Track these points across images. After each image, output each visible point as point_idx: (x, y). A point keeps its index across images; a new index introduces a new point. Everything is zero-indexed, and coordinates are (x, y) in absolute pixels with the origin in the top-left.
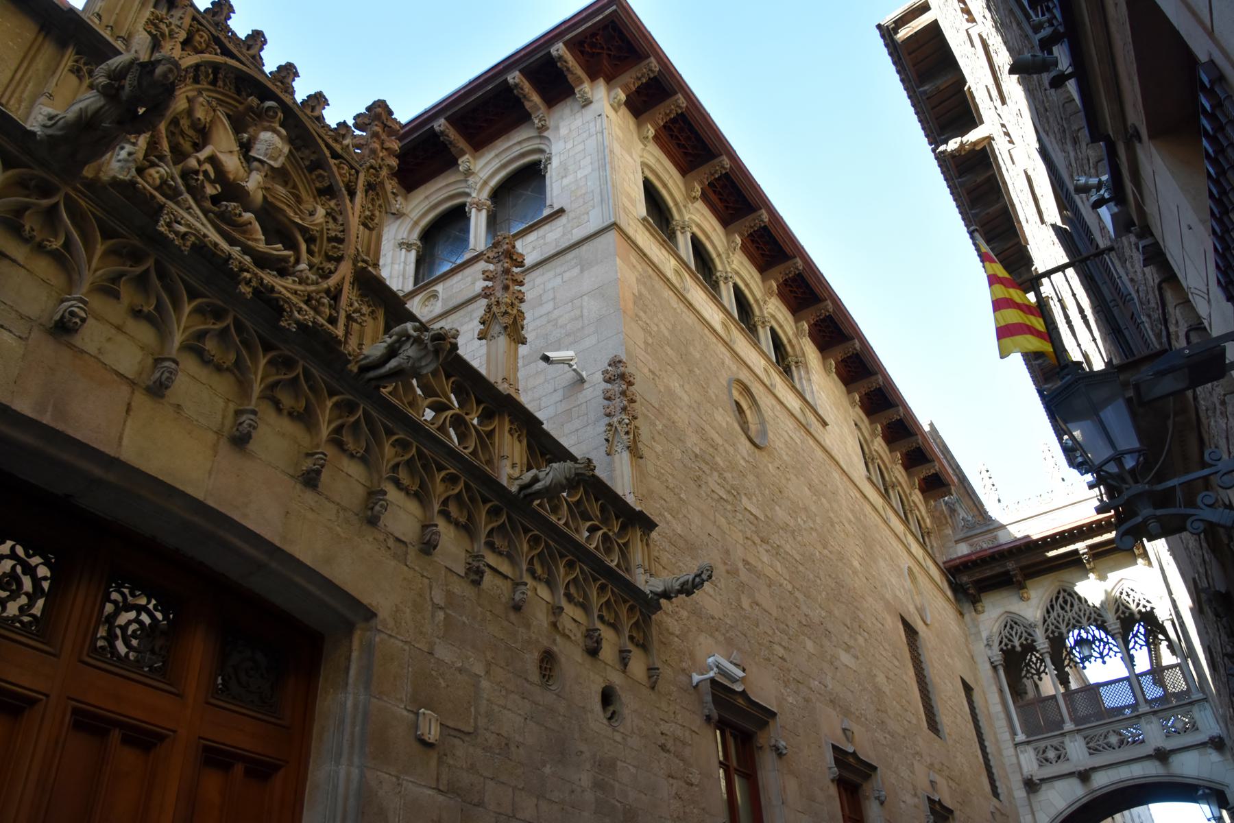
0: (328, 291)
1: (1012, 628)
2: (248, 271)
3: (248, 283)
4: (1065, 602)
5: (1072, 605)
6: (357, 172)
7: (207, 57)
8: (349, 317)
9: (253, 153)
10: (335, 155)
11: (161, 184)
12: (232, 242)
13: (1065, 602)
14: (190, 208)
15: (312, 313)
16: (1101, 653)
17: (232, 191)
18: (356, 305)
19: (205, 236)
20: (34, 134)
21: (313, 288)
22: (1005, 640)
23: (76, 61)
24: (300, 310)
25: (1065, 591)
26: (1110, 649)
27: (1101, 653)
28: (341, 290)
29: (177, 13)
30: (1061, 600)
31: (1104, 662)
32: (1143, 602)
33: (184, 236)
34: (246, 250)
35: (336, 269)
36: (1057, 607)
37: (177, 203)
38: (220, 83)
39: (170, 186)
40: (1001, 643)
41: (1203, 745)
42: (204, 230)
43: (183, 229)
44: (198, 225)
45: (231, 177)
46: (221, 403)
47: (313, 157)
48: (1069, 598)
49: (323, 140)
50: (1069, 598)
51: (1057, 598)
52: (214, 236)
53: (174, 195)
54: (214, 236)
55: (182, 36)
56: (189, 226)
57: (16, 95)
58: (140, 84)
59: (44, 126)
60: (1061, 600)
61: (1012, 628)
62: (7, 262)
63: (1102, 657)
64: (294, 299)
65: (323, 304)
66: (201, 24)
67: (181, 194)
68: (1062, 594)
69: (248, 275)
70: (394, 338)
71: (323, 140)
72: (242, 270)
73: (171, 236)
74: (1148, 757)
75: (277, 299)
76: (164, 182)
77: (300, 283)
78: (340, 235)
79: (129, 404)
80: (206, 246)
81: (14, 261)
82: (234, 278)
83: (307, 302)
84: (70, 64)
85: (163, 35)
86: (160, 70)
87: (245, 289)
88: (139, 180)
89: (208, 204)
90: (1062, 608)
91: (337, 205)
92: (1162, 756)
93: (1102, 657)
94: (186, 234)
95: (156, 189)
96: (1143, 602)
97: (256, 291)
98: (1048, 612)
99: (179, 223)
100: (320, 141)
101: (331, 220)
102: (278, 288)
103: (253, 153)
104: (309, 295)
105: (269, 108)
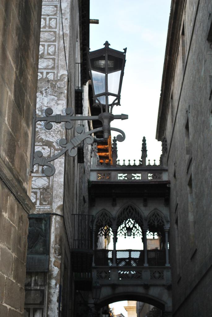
1: (104, 216)
4: (130, 211)
5: (132, 214)
13: (130, 211)
16: (134, 233)
22: (99, 221)
25: (131, 207)
26: (138, 232)
27: (134, 233)
30: (128, 210)
31: (134, 238)
32: (160, 221)
36: (126, 213)
40: (97, 222)
41: (164, 285)
48: (131, 210)
50: (131, 210)
51: (127, 209)
60: (128, 210)
61: (104, 216)
63: (134, 235)
68: (130, 208)
74: (141, 285)
90: (128, 214)
92: (147, 287)
93: (134, 235)
96: (160, 221)
98: (121, 214)
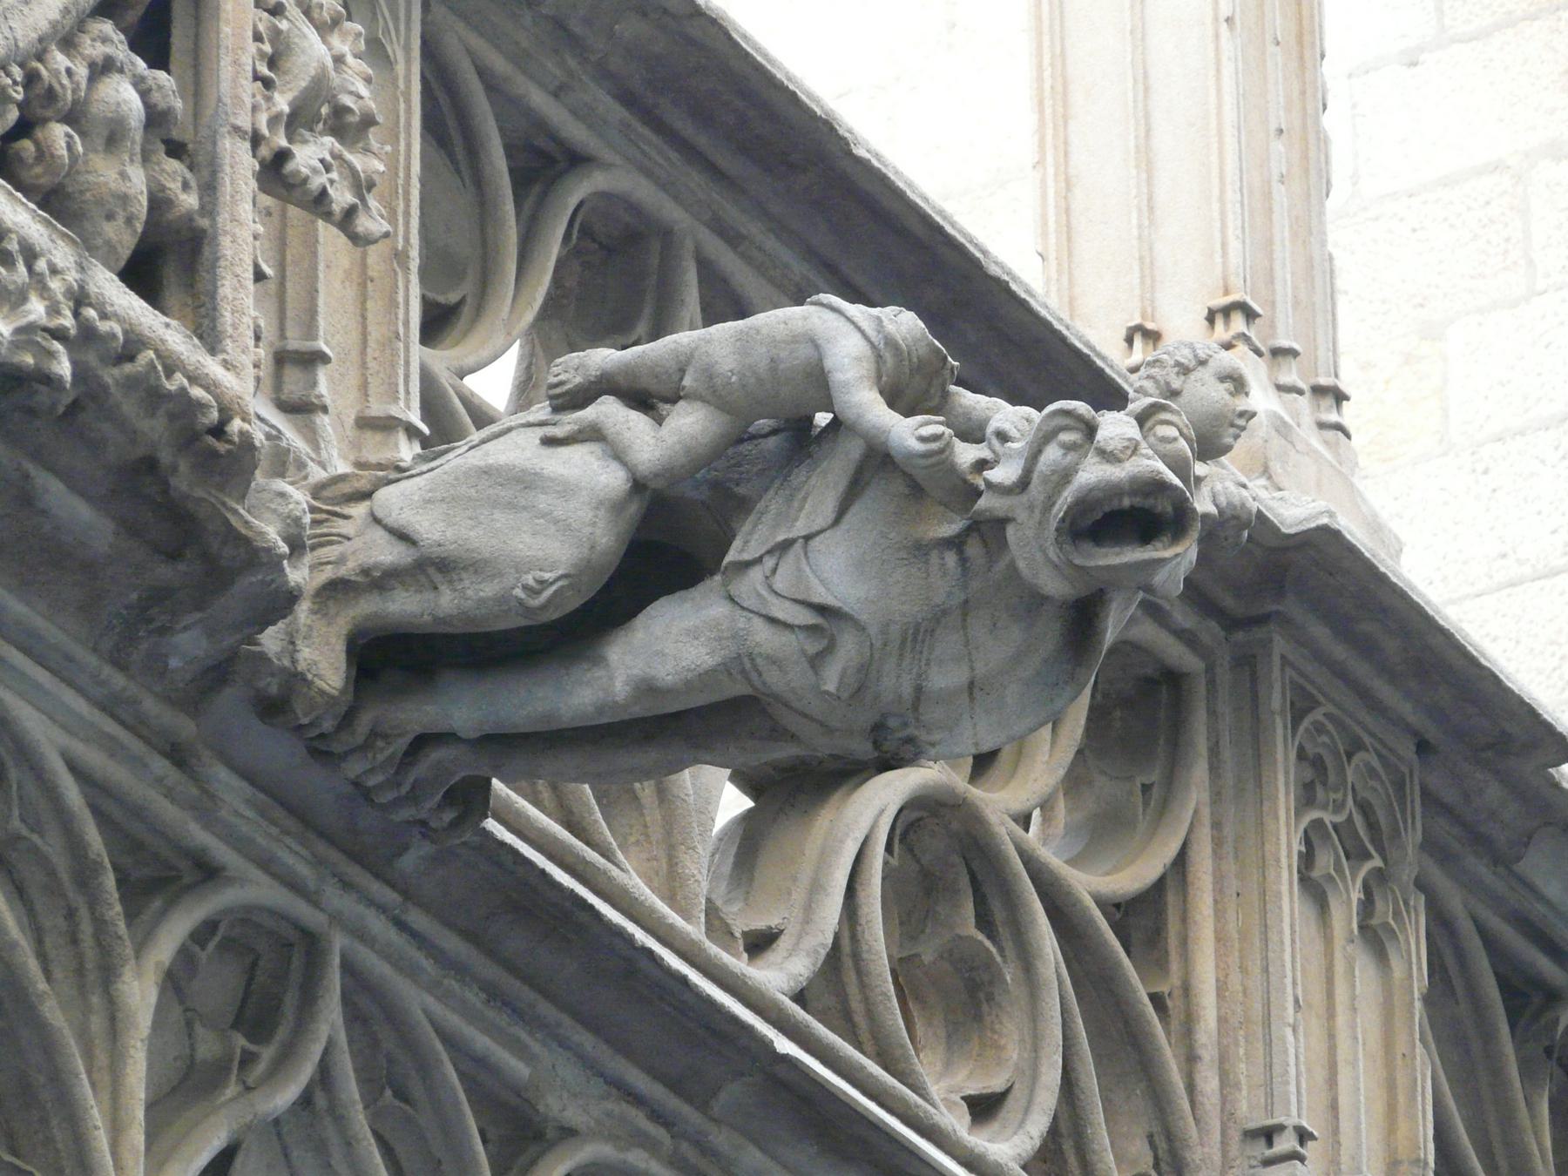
15: (60, 253)
18: (313, 50)
65: (113, 137)
70: (688, 424)
104: (31, 79)
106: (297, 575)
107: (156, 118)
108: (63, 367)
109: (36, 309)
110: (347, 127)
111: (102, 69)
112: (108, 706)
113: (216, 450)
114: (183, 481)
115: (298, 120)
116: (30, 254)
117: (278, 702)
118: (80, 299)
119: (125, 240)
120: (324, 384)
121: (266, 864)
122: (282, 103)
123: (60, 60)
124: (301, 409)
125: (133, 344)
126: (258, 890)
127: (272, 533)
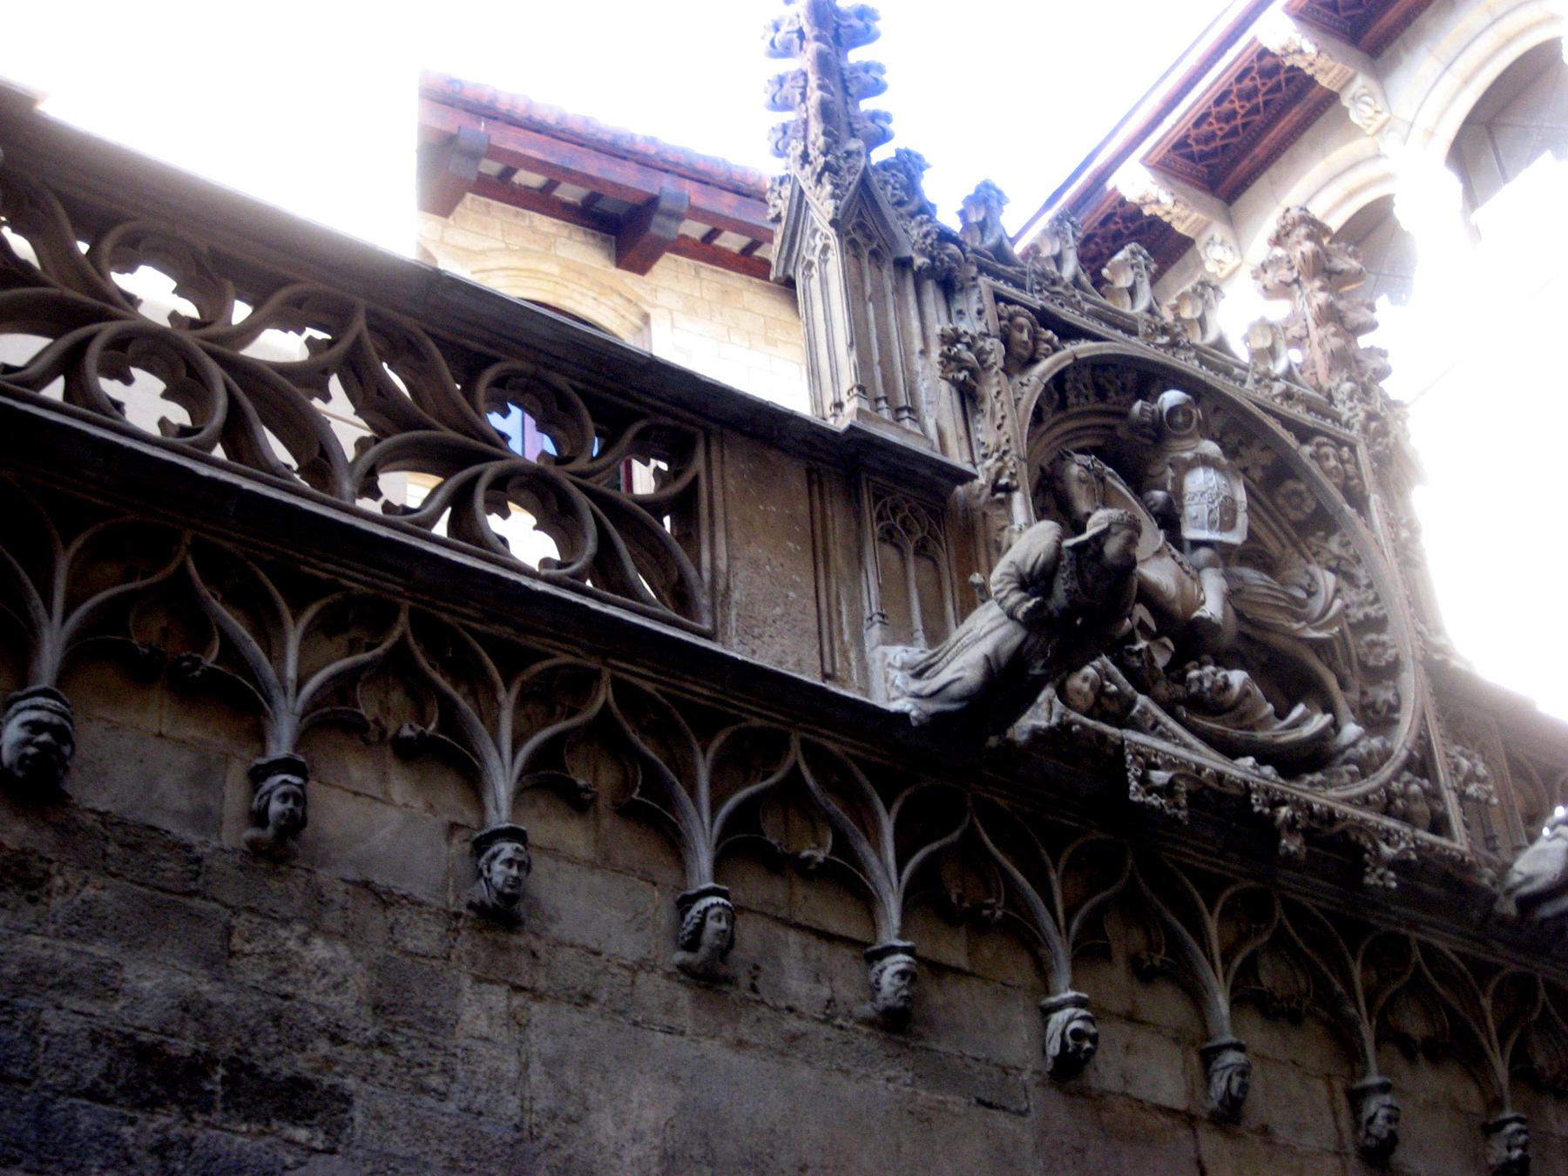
0: (1408, 765)
2: (1283, 803)
3: (1291, 825)
6: (1353, 449)
7: (1045, 367)
8: (1463, 797)
9: (1190, 533)
10: (1305, 434)
11: (1097, 702)
12: (1231, 750)
14: (1157, 723)
17: (1192, 638)
18: (1465, 764)
19: (1200, 769)
20: (903, 717)
21: (1386, 772)
23: (880, 518)
24: (1388, 835)
28: (1429, 744)
29: (970, 303)
33: (1168, 790)
34: (1266, 754)
35: (1397, 695)
37: (1136, 726)
38: (1072, 399)
39: (1111, 696)
42: (1196, 758)
43: (1160, 777)
44: (1182, 752)
45: (1178, 607)
46: (1319, 1085)
47: (1266, 458)
49: (1276, 415)
52: (1212, 761)
53: (1122, 714)
54: (1212, 761)
55: (995, 347)
56: (1169, 764)
57: (837, 645)
58: (1083, 585)
59: (917, 696)
62: (949, 978)
64: (1372, 817)
66: (1009, 301)
67: (1132, 702)
69: (1284, 811)
71: (1276, 415)
72: (1275, 804)
73: (1154, 800)
75: (1344, 833)
76: (1100, 691)
77: (1364, 775)
78: (1371, 611)
79: (1199, 1162)
80: (1205, 786)
81: (957, 971)
82: (1267, 829)
83: (1387, 811)
84: (877, 530)
85: (972, 371)
86: (1112, 547)
87: (1291, 844)
88: (1074, 715)
89: (1162, 689)
91: (1345, 545)
94: (1172, 782)
95: (1088, 715)
97: (1309, 836)
99: (1156, 767)
100: (1271, 422)
101: (1344, 585)
102: (1342, 809)
103: (1190, 533)
104: (1388, 791)
105: (1173, 410)
106: (1497, 890)
107: (1425, 791)
108: (1413, 856)
109: (1403, 845)
110: (1480, 780)
111: (1407, 784)
112: (1460, 934)
113: (1462, 865)
114: (1458, 875)
115: (1467, 782)
116: (1398, 832)
117: (1503, 921)
118: (1414, 840)
119: (1427, 823)
120: (1498, 843)
121: (1513, 961)
122: (1461, 778)
123: (1394, 785)
124: (1494, 850)
125: (1432, 846)
126: (1513, 968)
127: (1486, 882)
